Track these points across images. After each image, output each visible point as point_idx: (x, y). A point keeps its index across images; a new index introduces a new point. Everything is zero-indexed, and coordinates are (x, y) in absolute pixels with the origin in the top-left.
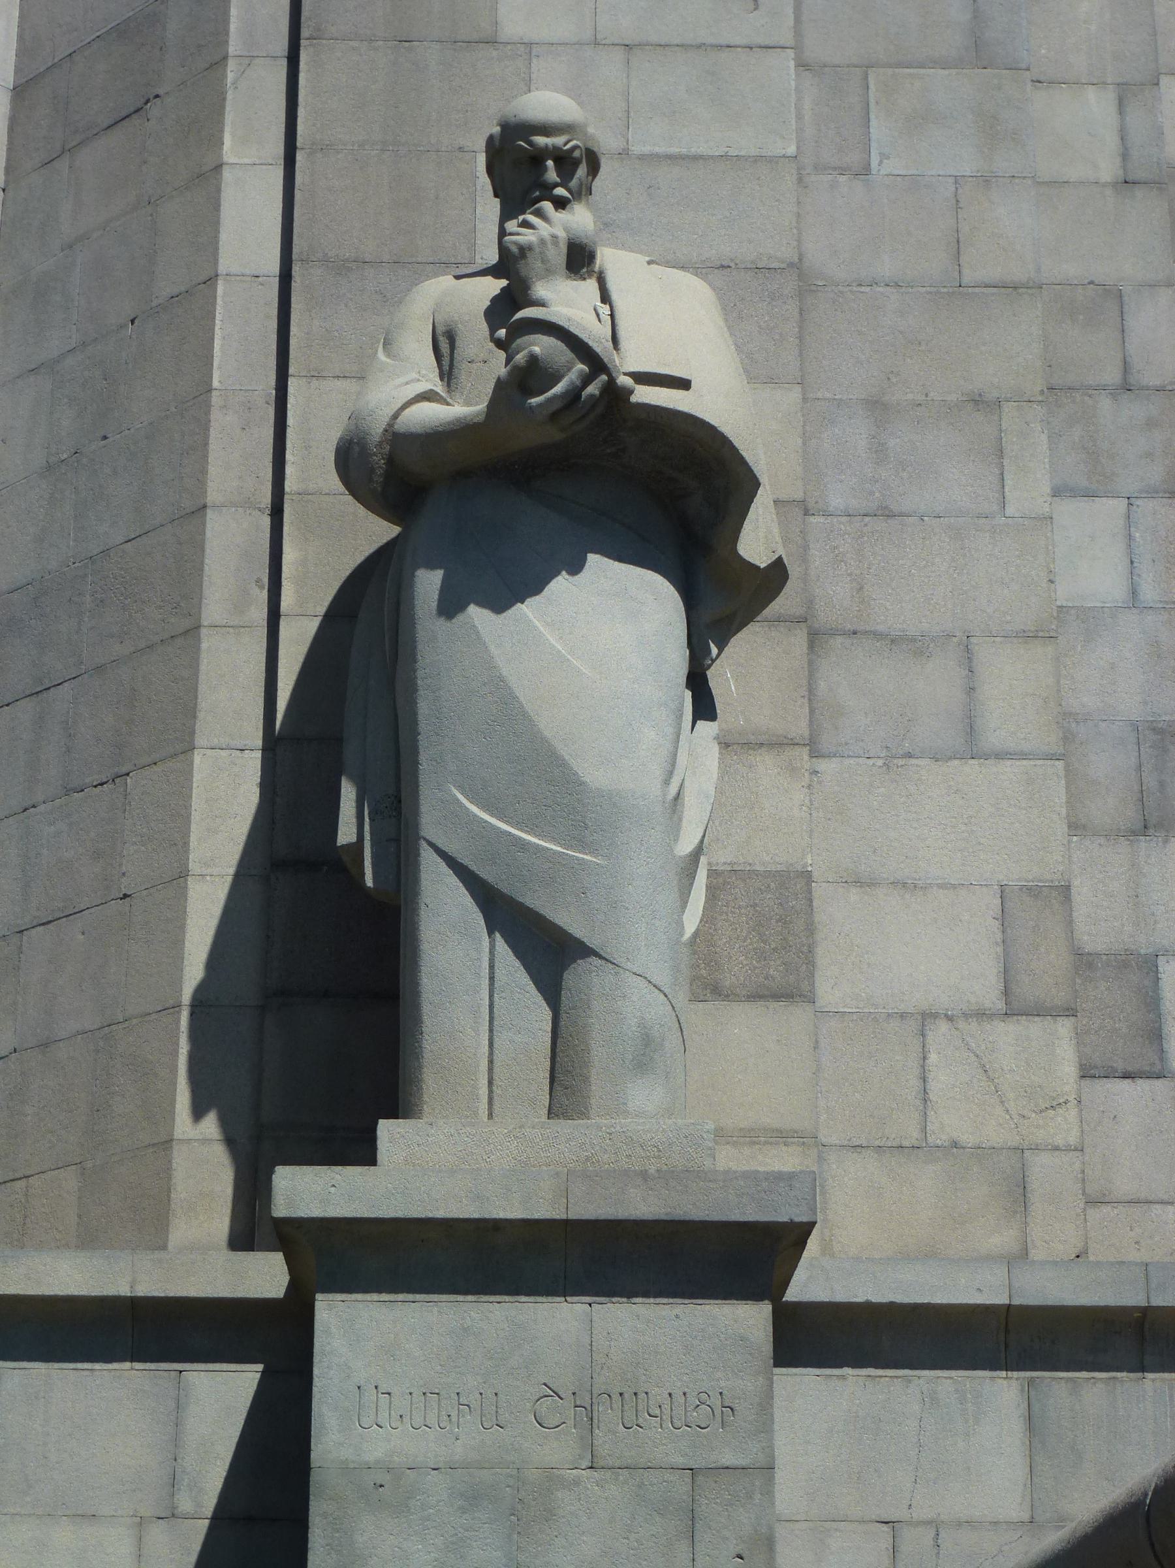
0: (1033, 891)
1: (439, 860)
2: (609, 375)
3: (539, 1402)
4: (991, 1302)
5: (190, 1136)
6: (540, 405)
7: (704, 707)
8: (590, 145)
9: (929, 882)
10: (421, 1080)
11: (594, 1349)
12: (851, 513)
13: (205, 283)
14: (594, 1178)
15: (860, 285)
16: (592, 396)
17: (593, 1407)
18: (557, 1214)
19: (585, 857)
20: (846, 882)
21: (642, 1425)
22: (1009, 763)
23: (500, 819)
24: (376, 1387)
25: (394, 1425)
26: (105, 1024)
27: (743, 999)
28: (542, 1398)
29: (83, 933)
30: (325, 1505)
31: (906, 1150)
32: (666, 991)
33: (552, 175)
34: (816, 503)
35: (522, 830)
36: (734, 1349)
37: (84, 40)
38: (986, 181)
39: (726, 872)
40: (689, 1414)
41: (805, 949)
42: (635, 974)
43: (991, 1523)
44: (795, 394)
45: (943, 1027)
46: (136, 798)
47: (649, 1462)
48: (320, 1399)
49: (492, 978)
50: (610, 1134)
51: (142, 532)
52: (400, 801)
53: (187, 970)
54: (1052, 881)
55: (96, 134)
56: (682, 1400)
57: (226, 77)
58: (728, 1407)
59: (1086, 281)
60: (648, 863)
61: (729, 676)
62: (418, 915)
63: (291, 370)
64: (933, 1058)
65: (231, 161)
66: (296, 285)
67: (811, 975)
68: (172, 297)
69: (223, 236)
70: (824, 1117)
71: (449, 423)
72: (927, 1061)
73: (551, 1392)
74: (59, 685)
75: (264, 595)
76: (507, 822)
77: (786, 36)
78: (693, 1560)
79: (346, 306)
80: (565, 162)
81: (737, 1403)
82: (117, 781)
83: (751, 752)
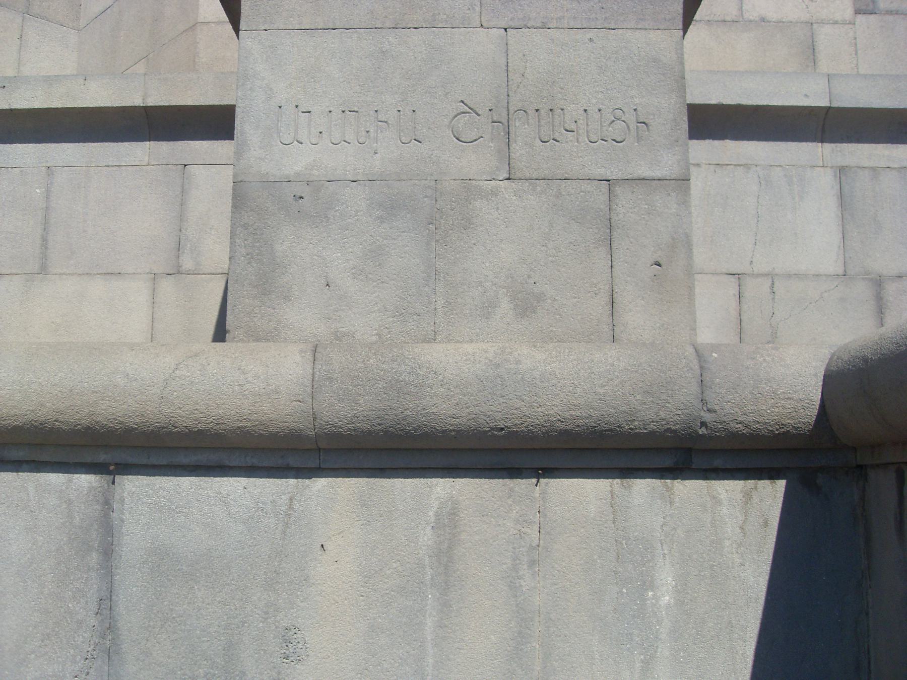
3: (456, 118)
4: (816, 105)
11: (510, 69)
21: (558, 139)
28: (459, 114)
30: (246, 217)
31: (728, 23)
36: (646, 70)
40: (604, 128)
43: (814, 275)
47: (566, 173)
48: (242, 118)
56: (597, 116)
58: (644, 123)
78: (612, 267)
81: (652, 119)
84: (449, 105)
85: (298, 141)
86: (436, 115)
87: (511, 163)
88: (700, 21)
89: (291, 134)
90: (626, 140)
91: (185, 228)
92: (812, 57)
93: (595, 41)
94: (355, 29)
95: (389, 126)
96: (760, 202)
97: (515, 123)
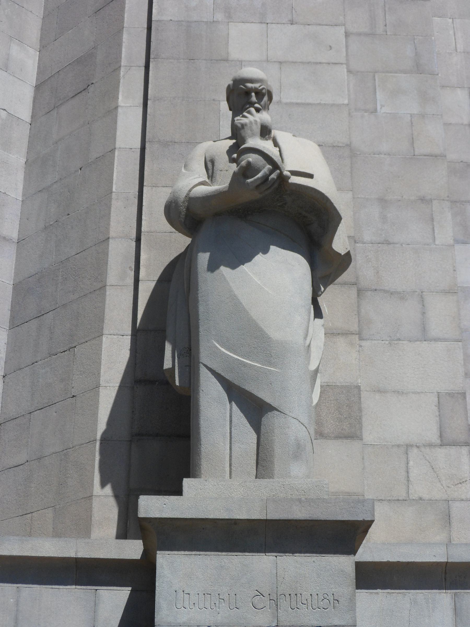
0: (451, 395)
1: (208, 372)
2: (280, 170)
5: (100, 495)
6: (252, 182)
7: (318, 313)
8: (269, 89)
9: (408, 391)
10: (201, 464)
11: (278, 575)
12: (373, 243)
13: (110, 152)
14: (278, 502)
15: (374, 154)
16: (273, 179)
17: (278, 600)
18: (263, 517)
19: (271, 369)
20: (374, 391)
22: (440, 343)
23: (234, 354)
24: (183, 591)
25: (191, 608)
26: (65, 449)
27: (333, 438)
28: (255, 596)
29: (56, 412)
31: (400, 501)
32: (306, 426)
33: (254, 99)
34: (359, 238)
35: (244, 358)
36: (338, 576)
37: (64, 66)
38: (423, 116)
39: (325, 386)
40: (319, 603)
41: (358, 418)
42: (293, 418)
44: (350, 195)
45: (415, 450)
46: (79, 356)
48: (159, 596)
49: (231, 421)
50: (284, 485)
51: (83, 250)
52: (191, 350)
53: (99, 425)
54: (458, 391)
55: (68, 100)
56: (316, 597)
57: (120, 74)
59: (460, 161)
60: (298, 371)
61: (325, 306)
62: (199, 395)
63: (145, 184)
64: (411, 463)
65: (122, 105)
66: (147, 151)
67: (361, 428)
68: (97, 158)
69: (118, 133)
70: (366, 488)
71: (212, 192)
72: (409, 465)
73: (259, 594)
74: (47, 313)
75: (133, 273)
76: (237, 355)
77: (343, 60)
79: (167, 159)
80: (259, 94)
82: (71, 350)
83: (334, 337)
84: (251, 592)
85: (183, 607)
86: (245, 596)
87: (278, 619)
88: (385, 500)
89: (181, 604)
90: (329, 608)
91: (97, 625)
92: (448, 521)
93: (316, 562)
94: (209, 555)
95: (224, 601)
96: (411, 613)
97: (280, 600)
